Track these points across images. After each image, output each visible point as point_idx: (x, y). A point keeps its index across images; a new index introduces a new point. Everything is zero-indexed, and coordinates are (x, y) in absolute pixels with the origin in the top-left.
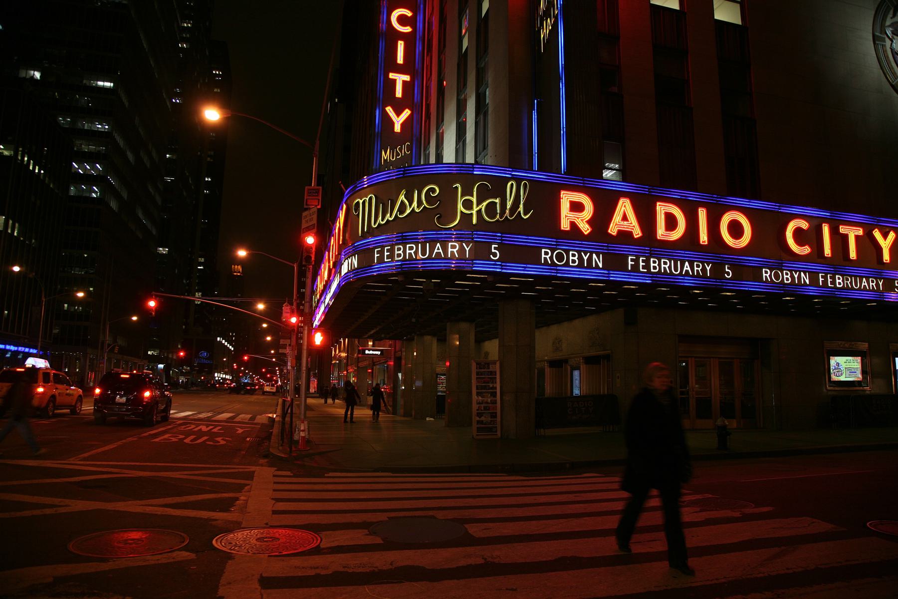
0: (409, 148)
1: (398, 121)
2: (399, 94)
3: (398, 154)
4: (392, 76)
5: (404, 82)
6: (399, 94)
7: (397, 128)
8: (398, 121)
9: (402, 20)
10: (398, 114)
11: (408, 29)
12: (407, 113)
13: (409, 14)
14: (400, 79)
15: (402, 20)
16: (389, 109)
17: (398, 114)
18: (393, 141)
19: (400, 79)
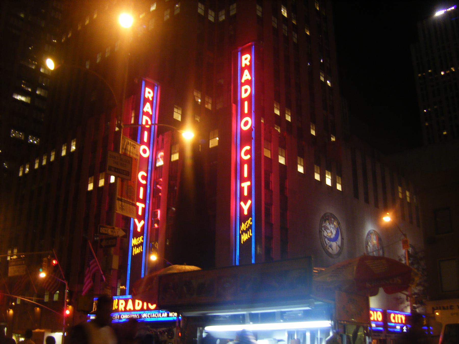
0: (143, 239)
1: (140, 225)
2: (140, 213)
3: (138, 242)
4: (138, 204)
5: (143, 208)
6: (140, 213)
7: (139, 230)
8: (140, 225)
9: (143, 177)
10: (139, 222)
11: (144, 182)
12: (142, 222)
13: (145, 175)
14: (141, 206)
15: (143, 177)
16: (136, 220)
17: (139, 222)
18: (137, 235)
19: (141, 206)
